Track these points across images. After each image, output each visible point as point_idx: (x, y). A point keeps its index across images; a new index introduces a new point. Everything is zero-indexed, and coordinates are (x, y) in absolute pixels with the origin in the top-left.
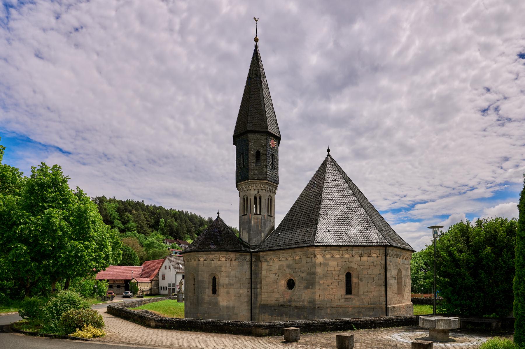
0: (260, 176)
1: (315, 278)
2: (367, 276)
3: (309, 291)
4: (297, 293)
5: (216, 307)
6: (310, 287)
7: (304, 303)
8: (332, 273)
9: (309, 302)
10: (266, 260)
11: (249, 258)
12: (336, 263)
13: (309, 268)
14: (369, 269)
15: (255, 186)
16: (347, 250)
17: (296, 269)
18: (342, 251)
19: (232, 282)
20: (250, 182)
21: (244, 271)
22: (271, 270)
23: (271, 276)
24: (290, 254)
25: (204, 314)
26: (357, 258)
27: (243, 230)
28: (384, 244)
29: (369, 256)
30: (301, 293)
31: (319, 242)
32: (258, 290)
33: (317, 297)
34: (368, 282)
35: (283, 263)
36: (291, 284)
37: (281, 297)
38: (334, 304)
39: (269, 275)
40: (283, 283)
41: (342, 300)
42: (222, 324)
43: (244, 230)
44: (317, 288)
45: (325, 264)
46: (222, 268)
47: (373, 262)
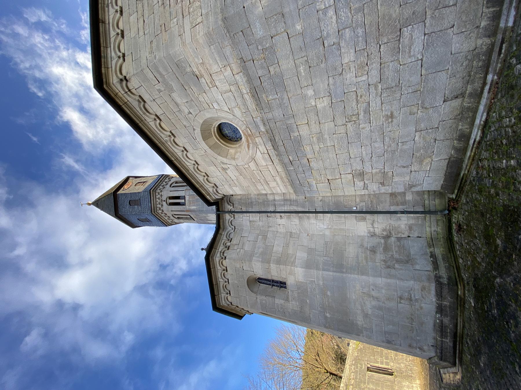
5: (309, 290)
11: (228, 216)
15: (159, 206)
19: (261, 250)
20: (154, 212)
25: (326, 317)
32: (277, 198)
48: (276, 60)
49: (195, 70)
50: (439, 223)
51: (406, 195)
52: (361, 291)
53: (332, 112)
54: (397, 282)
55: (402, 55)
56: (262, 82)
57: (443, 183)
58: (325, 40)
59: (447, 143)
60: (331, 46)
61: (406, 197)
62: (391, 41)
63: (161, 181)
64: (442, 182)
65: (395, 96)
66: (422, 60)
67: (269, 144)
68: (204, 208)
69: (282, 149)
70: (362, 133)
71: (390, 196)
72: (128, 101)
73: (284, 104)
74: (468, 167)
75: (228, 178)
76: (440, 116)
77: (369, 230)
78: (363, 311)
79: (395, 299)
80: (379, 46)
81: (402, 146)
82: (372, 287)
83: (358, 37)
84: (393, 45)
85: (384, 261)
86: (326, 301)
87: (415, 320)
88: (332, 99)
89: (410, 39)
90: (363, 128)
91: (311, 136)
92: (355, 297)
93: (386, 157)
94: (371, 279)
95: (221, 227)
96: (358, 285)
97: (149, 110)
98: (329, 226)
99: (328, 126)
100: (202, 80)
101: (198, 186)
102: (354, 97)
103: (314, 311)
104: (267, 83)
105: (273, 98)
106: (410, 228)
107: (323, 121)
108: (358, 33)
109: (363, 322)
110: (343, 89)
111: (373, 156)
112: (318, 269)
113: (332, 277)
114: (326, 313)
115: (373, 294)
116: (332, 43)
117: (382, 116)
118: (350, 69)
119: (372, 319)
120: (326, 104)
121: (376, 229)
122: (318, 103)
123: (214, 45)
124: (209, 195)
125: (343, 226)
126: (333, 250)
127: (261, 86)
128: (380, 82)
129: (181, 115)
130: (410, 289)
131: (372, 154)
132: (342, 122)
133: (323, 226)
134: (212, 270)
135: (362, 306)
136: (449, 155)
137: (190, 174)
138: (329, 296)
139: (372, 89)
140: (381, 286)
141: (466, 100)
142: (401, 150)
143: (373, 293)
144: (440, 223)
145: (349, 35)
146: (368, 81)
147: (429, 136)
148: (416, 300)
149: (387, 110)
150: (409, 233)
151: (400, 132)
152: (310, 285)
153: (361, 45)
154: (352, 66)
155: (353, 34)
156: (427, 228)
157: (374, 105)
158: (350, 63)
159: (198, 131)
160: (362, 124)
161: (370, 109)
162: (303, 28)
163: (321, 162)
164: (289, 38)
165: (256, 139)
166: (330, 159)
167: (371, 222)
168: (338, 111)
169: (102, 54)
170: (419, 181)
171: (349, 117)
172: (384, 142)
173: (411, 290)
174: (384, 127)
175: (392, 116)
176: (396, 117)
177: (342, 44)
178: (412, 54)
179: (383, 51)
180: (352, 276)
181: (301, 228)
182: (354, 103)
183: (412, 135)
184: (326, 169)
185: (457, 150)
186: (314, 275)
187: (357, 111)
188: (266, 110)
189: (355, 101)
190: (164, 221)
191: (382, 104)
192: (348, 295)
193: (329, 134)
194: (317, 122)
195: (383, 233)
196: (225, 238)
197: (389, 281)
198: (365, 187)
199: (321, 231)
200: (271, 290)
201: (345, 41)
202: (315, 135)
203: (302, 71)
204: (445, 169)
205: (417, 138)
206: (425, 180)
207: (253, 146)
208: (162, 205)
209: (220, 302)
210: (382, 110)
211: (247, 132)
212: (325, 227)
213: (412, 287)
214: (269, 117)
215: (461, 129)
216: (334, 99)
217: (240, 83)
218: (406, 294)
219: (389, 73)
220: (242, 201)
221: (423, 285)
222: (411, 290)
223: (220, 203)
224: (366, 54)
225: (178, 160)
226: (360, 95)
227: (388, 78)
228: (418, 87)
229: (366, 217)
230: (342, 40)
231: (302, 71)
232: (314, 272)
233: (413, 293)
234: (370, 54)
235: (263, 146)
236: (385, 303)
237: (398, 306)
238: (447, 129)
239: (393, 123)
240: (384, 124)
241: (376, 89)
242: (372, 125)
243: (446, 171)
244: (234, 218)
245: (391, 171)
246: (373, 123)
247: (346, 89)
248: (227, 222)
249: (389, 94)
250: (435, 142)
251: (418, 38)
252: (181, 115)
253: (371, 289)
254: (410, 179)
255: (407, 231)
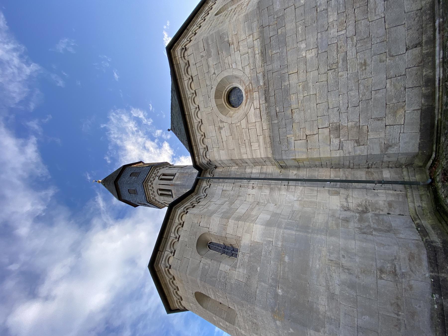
5: (263, 253)
6: (226, 39)
20: (145, 183)
25: (276, 295)
37: (252, 109)
48: (284, 24)
49: (230, 39)
50: (423, 198)
51: (383, 173)
52: (328, 257)
53: (317, 61)
54: (376, 247)
55: (370, 14)
56: (271, 40)
57: (419, 141)
58: (318, 8)
59: (416, 91)
60: (321, 11)
61: (384, 175)
62: (362, 6)
63: (163, 165)
64: (418, 141)
65: (367, 45)
66: (384, 17)
67: (263, 98)
68: (187, 183)
69: (272, 99)
70: (340, 80)
71: (366, 173)
72: (180, 63)
73: (283, 56)
74: (440, 111)
75: (220, 140)
76: (405, 63)
77: (343, 205)
78: (328, 288)
79: (374, 272)
80: (353, 9)
81: (375, 94)
82: (342, 253)
83: (340, 4)
84: (363, 8)
85: (359, 228)
86: (282, 270)
87: (402, 308)
88: (319, 50)
89: (375, 3)
90: (341, 76)
91: (298, 84)
92: (319, 265)
93: (360, 107)
94: (342, 242)
95: (195, 191)
96: (324, 249)
97: (189, 72)
98: (299, 198)
99: (313, 74)
100: (232, 46)
101: (193, 144)
102: (335, 47)
103: (263, 284)
104: (275, 41)
105: (275, 52)
106: (390, 205)
107: (309, 70)
108: (340, 2)
109: (326, 306)
110: (327, 41)
111: (349, 106)
112: (279, 227)
113: (294, 237)
114: (277, 289)
115: (343, 262)
116: (323, 9)
117: (357, 63)
118: (333, 26)
119: (340, 304)
120: (313, 55)
121: (349, 204)
122: (308, 54)
123: (248, 22)
124: (198, 156)
125: (314, 199)
126: (300, 216)
127: (270, 44)
128: (355, 35)
129: (208, 75)
130: (394, 258)
131: (348, 103)
132: (325, 70)
133: (293, 197)
134: (170, 220)
135: (327, 280)
136: (421, 105)
137: (192, 131)
138: (286, 262)
139: (349, 41)
140: (354, 251)
141: (423, 48)
142: (375, 99)
143: (343, 261)
144: (424, 198)
145: (334, 4)
146: (346, 34)
147: (399, 83)
148: (403, 275)
149: (361, 58)
150: (389, 210)
151: (373, 80)
152: (266, 247)
153: (342, 9)
154: (335, 23)
155: (336, 2)
156: (410, 204)
157: (351, 54)
158: (334, 22)
159: (214, 88)
160: (340, 72)
161: (348, 58)
162: (305, 2)
163: (302, 113)
164: (295, 9)
165: (254, 93)
166: (311, 110)
167: (345, 196)
168: (322, 61)
169: (179, 39)
170: (394, 139)
171: (331, 65)
172: (359, 91)
173: (396, 259)
174: (359, 74)
175: (365, 64)
176: (369, 65)
177: (329, 9)
178: (377, 13)
179: (357, 12)
180: (319, 236)
181: (269, 199)
182: (335, 53)
183: (384, 82)
184: (306, 121)
185: (426, 96)
186: (274, 233)
187: (337, 60)
188: (268, 63)
189: (336, 51)
190: (148, 195)
191: (357, 53)
192: (311, 263)
193: (313, 83)
194: (304, 71)
195: (358, 208)
196: (194, 199)
197: (364, 245)
198: (341, 147)
199: (290, 203)
200: (219, 256)
201: (331, 7)
202: (302, 83)
203: (300, 30)
204: (419, 122)
205: (388, 86)
206: (400, 138)
207: (250, 101)
208: (154, 179)
209: (159, 262)
210: (357, 59)
211: (249, 87)
212: (295, 199)
213: (396, 254)
214: (269, 68)
215: (426, 75)
216: (320, 50)
217: (256, 46)
218: (389, 265)
219: (362, 27)
220: (223, 173)
221: (411, 253)
222: (396, 259)
223: (203, 171)
224: (345, 15)
225: (190, 116)
226: (339, 46)
227: (361, 32)
228: (385, 38)
229: (340, 191)
230: (329, 7)
231: (300, 30)
232: (275, 230)
233: (397, 264)
234: (348, 15)
235: (258, 101)
236: (359, 277)
237: (377, 283)
238: (414, 76)
239: (367, 70)
240: (359, 72)
241: (352, 41)
242: (348, 73)
243: (420, 125)
244: (209, 187)
245: (366, 124)
246: (349, 71)
247: (330, 41)
248: (202, 189)
249: (362, 44)
250: (405, 91)
251: (380, 3)
252: (208, 75)
253: (341, 256)
254: (385, 136)
255: (386, 208)
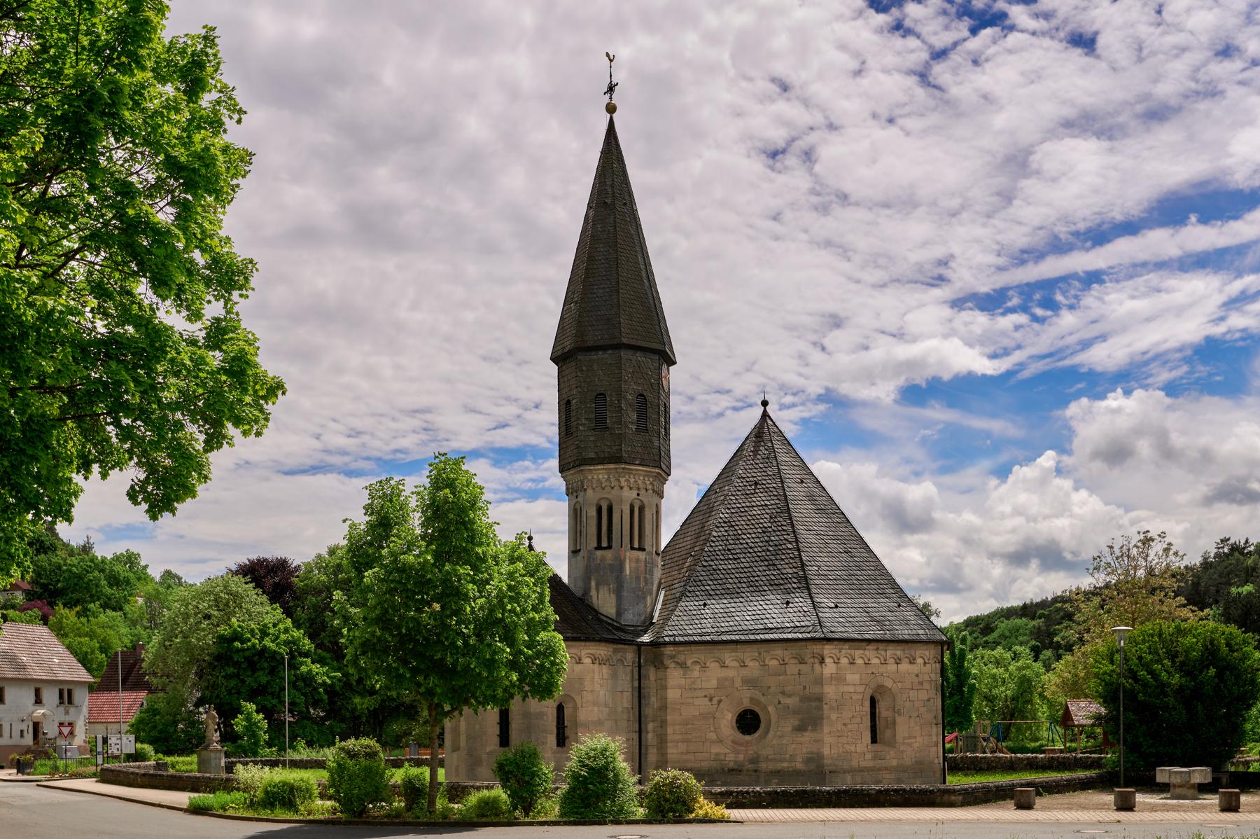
0: (646, 456)
1: (821, 709)
2: (908, 704)
3: (807, 736)
4: (774, 742)
7: (793, 764)
8: (851, 698)
9: (808, 761)
10: (683, 665)
12: (857, 676)
13: (805, 688)
14: (912, 689)
16: (877, 649)
17: (769, 687)
18: (870, 652)
20: (623, 468)
21: (620, 689)
22: (695, 689)
23: (697, 702)
24: (756, 654)
26: (892, 667)
27: (597, 585)
28: (939, 638)
29: (912, 661)
30: (784, 742)
31: (831, 632)
33: (826, 751)
34: (910, 717)
35: (731, 673)
36: (748, 722)
37: (727, 751)
38: (855, 763)
39: (691, 701)
40: (728, 719)
41: (869, 756)
42: (873, 792)
43: (600, 587)
44: (826, 729)
45: (839, 679)
46: (586, 683)
47: (917, 676)
159: (763, 699)
235: (732, 759)
